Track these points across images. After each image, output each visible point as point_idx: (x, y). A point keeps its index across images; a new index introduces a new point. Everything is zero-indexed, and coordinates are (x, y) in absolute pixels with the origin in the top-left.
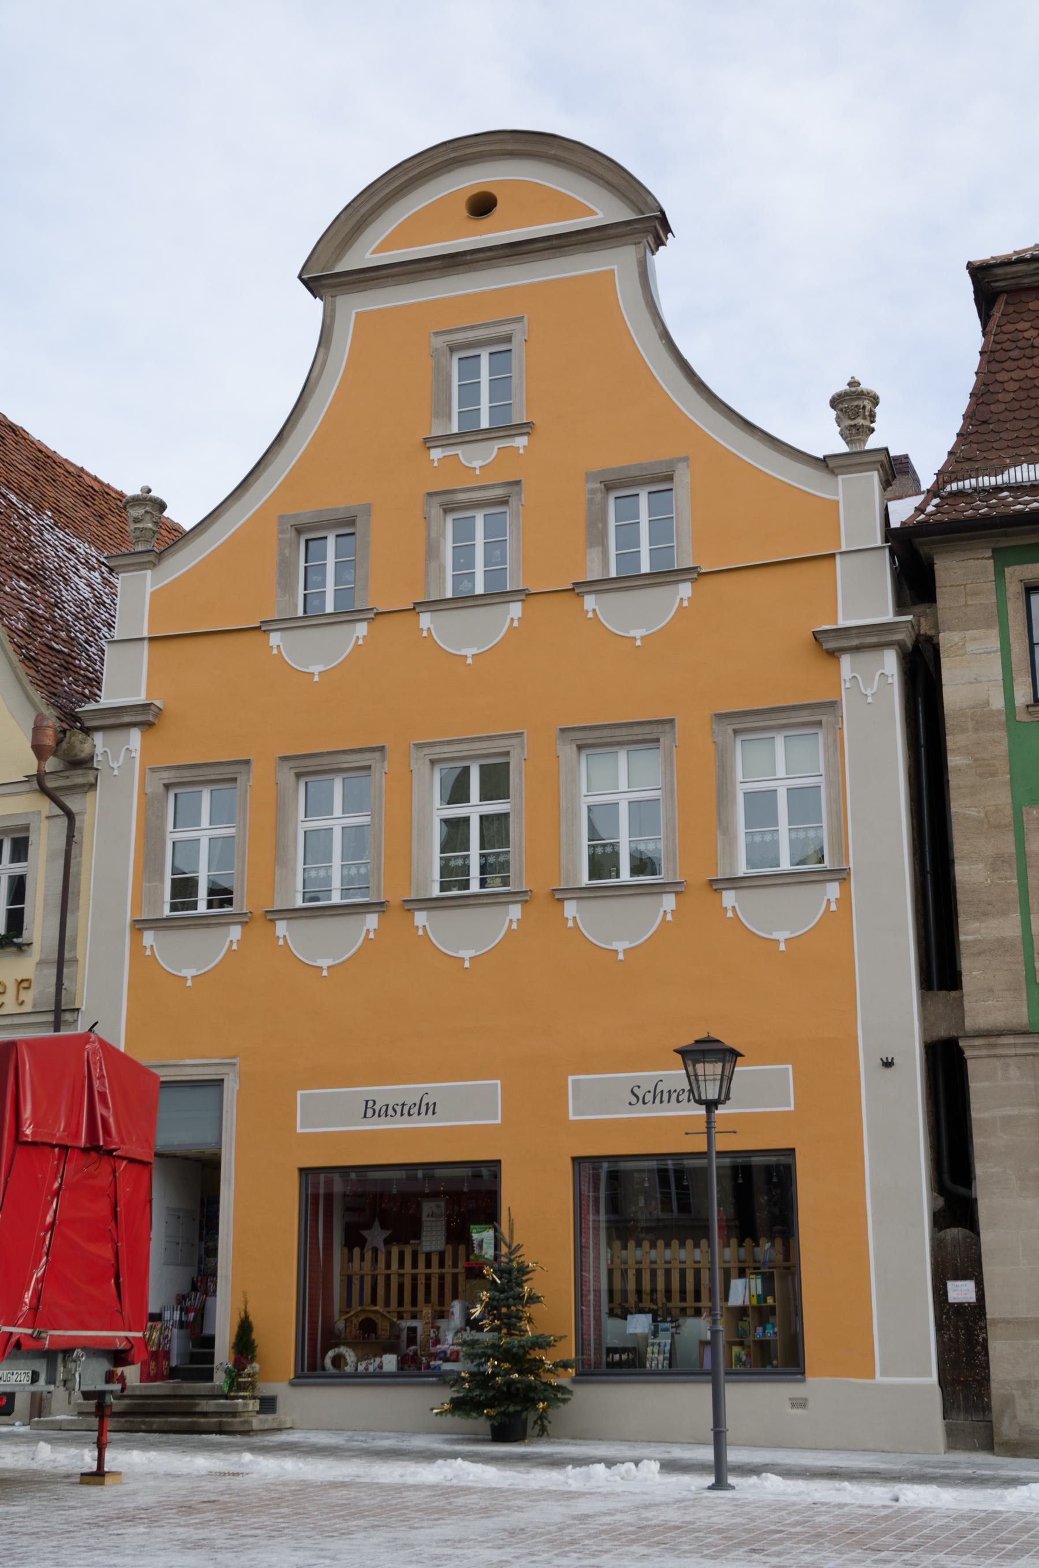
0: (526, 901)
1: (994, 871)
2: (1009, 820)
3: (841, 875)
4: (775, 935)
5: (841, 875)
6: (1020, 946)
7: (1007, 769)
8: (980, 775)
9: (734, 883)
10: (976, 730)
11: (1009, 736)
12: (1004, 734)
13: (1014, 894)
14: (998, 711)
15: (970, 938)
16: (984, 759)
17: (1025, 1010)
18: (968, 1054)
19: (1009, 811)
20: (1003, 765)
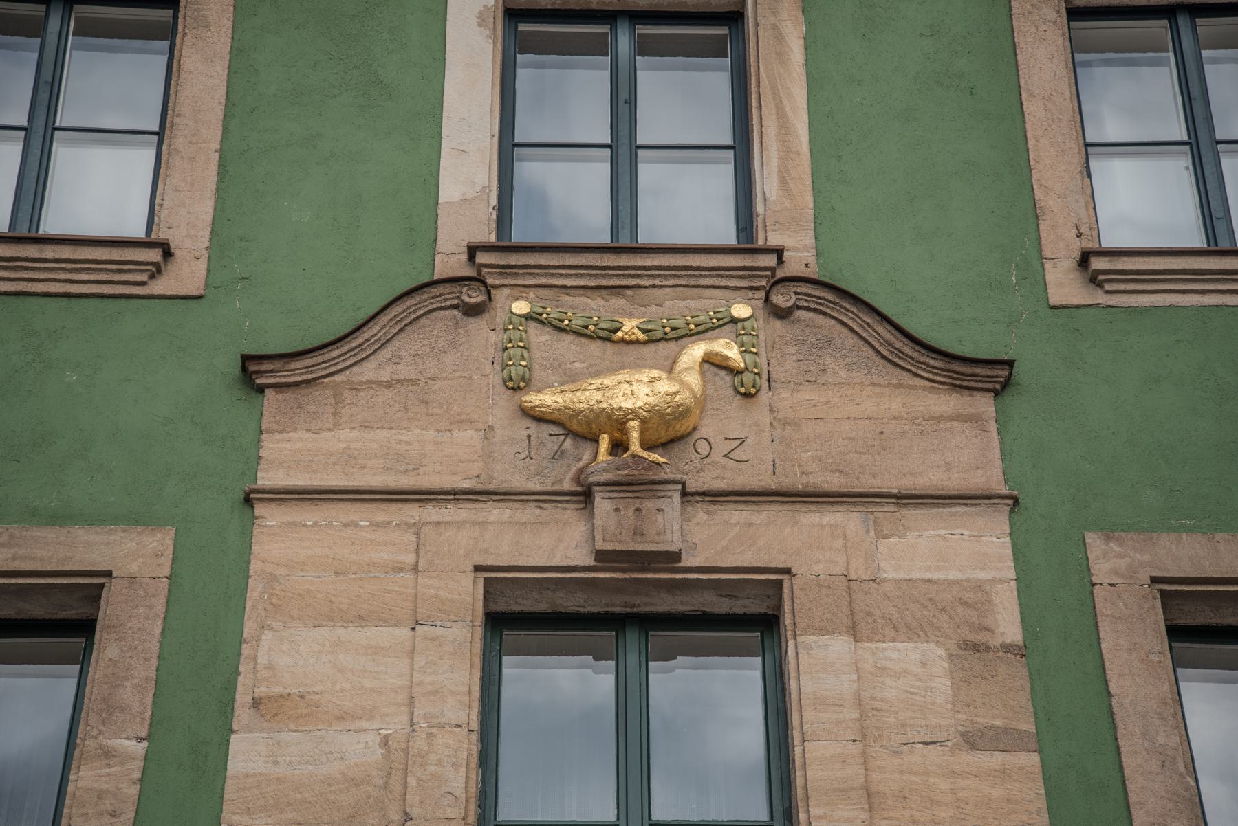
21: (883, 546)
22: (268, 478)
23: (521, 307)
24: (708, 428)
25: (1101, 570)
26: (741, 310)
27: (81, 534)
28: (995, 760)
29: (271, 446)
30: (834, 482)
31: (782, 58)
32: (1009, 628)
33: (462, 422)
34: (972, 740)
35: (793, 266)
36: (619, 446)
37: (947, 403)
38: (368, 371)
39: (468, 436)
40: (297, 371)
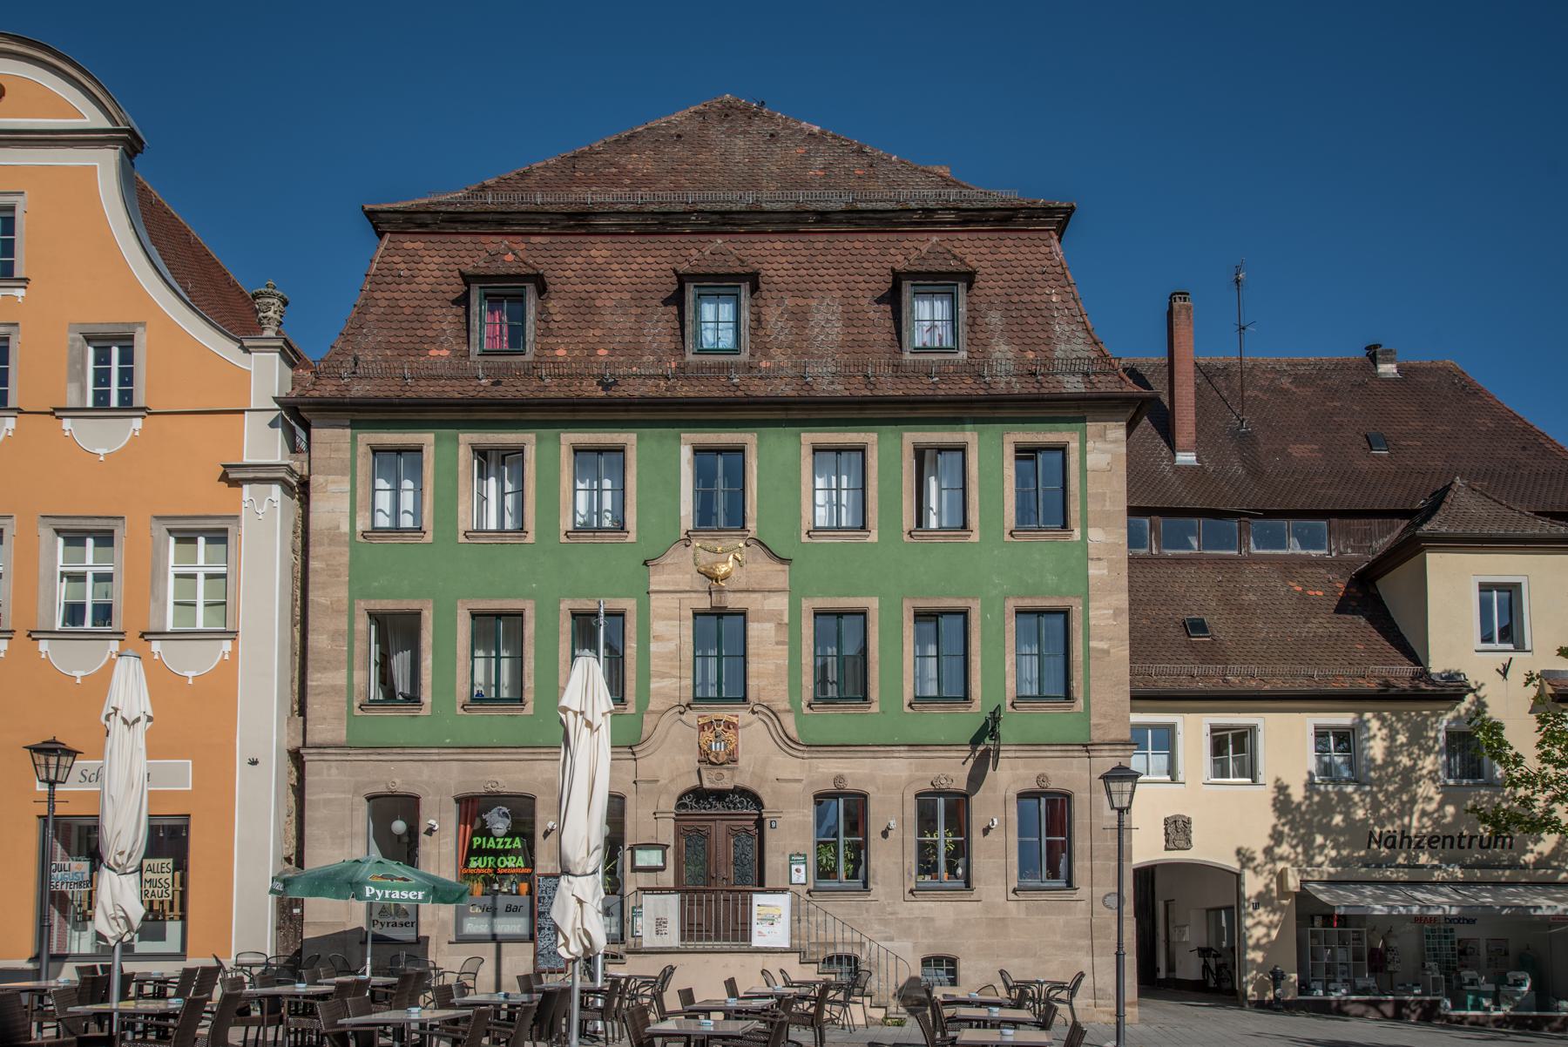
0: (11, 638)
1: (333, 640)
2: (346, 607)
3: (232, 635)
4: (186, 673)
5: (232, 635)
6: (345, 691)
7: (347, 573)
8: (330, 576)
9: (161, 634)
10: (330, 545)
11: (351, 551)
12: (347, 549)
13: (344, 657)
14: (345, 533)
15: (314, 683)
16: (332, 565)
17: (345, 732)
18: (306, 758)
19: (346, 601)
20: (345, 571)
21: (767, 601)
22: (652, 587)
23: (698, 545)
24: (733, 574)
25: (804, 606)
26: (741, 545)
27: (620, 600)
28: (780, 647)
29: (652, 579)
30: (757, 587)
31: (752, 473)
32: (786, 620)
33: (687, 573)
34: (777, 643)
35: (750, 535)
36: (717, 581)
37: (780, 567)
38: (669, 561)
39: (688, 576)
40: (655, 562)
